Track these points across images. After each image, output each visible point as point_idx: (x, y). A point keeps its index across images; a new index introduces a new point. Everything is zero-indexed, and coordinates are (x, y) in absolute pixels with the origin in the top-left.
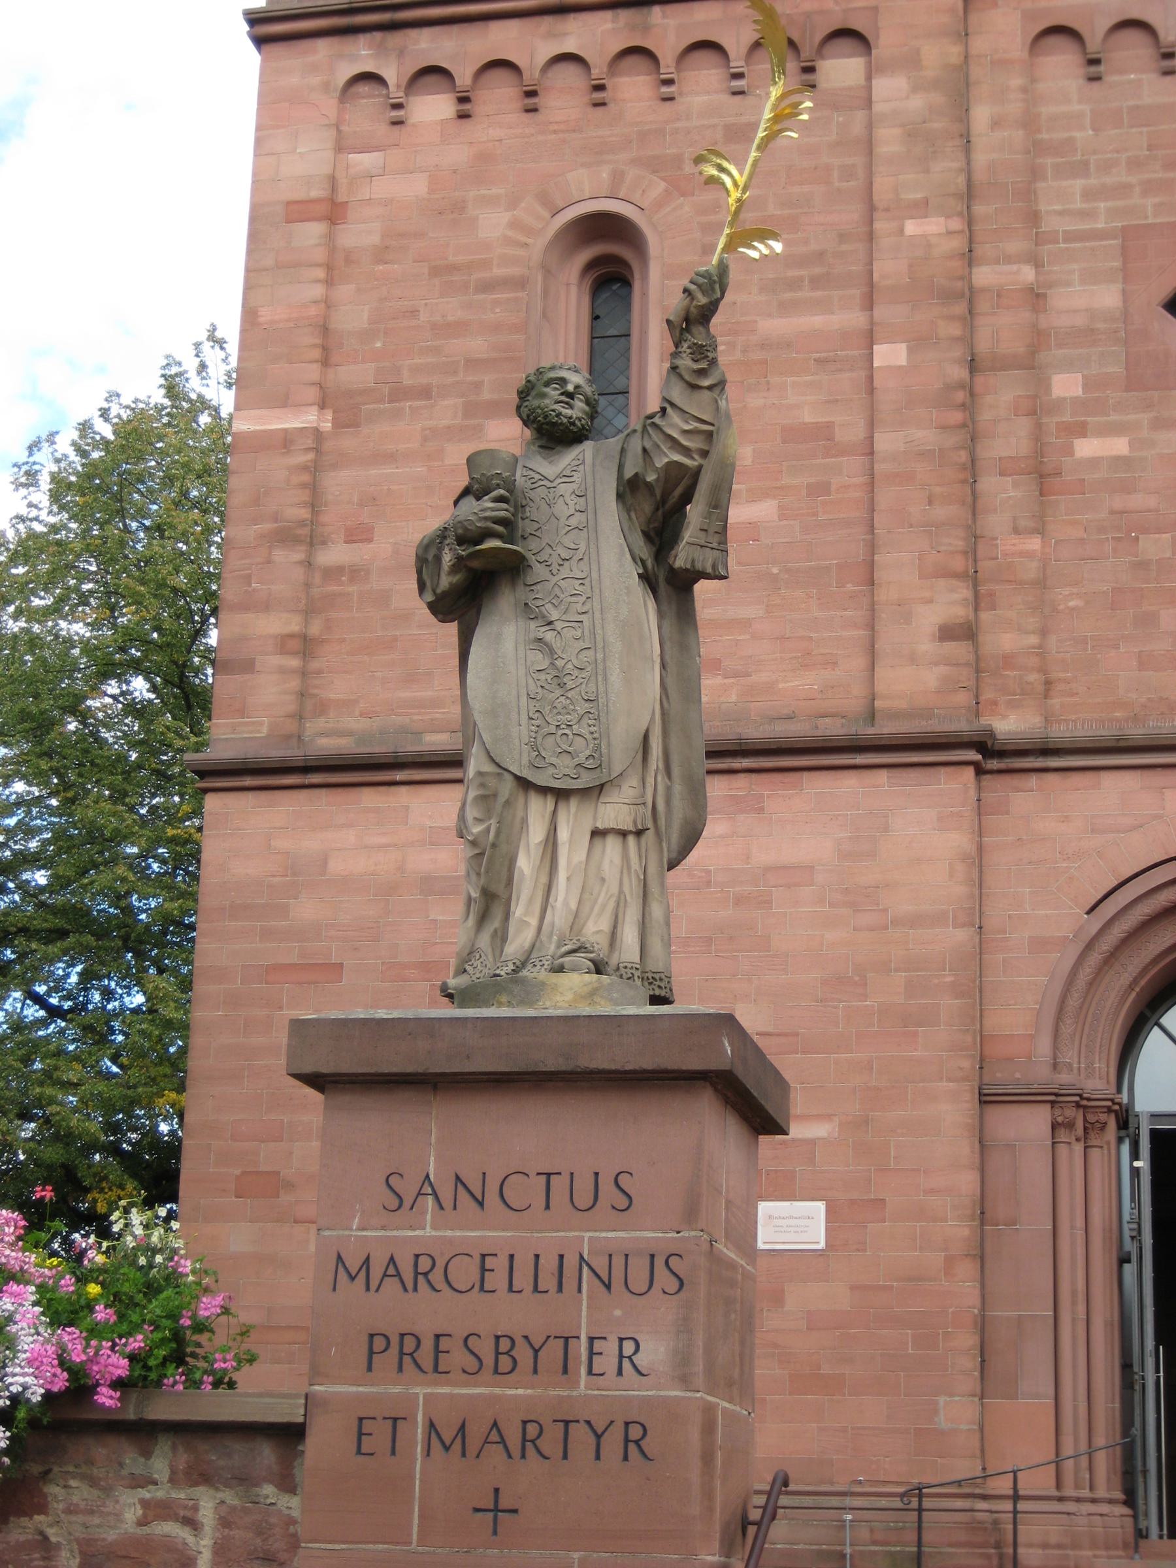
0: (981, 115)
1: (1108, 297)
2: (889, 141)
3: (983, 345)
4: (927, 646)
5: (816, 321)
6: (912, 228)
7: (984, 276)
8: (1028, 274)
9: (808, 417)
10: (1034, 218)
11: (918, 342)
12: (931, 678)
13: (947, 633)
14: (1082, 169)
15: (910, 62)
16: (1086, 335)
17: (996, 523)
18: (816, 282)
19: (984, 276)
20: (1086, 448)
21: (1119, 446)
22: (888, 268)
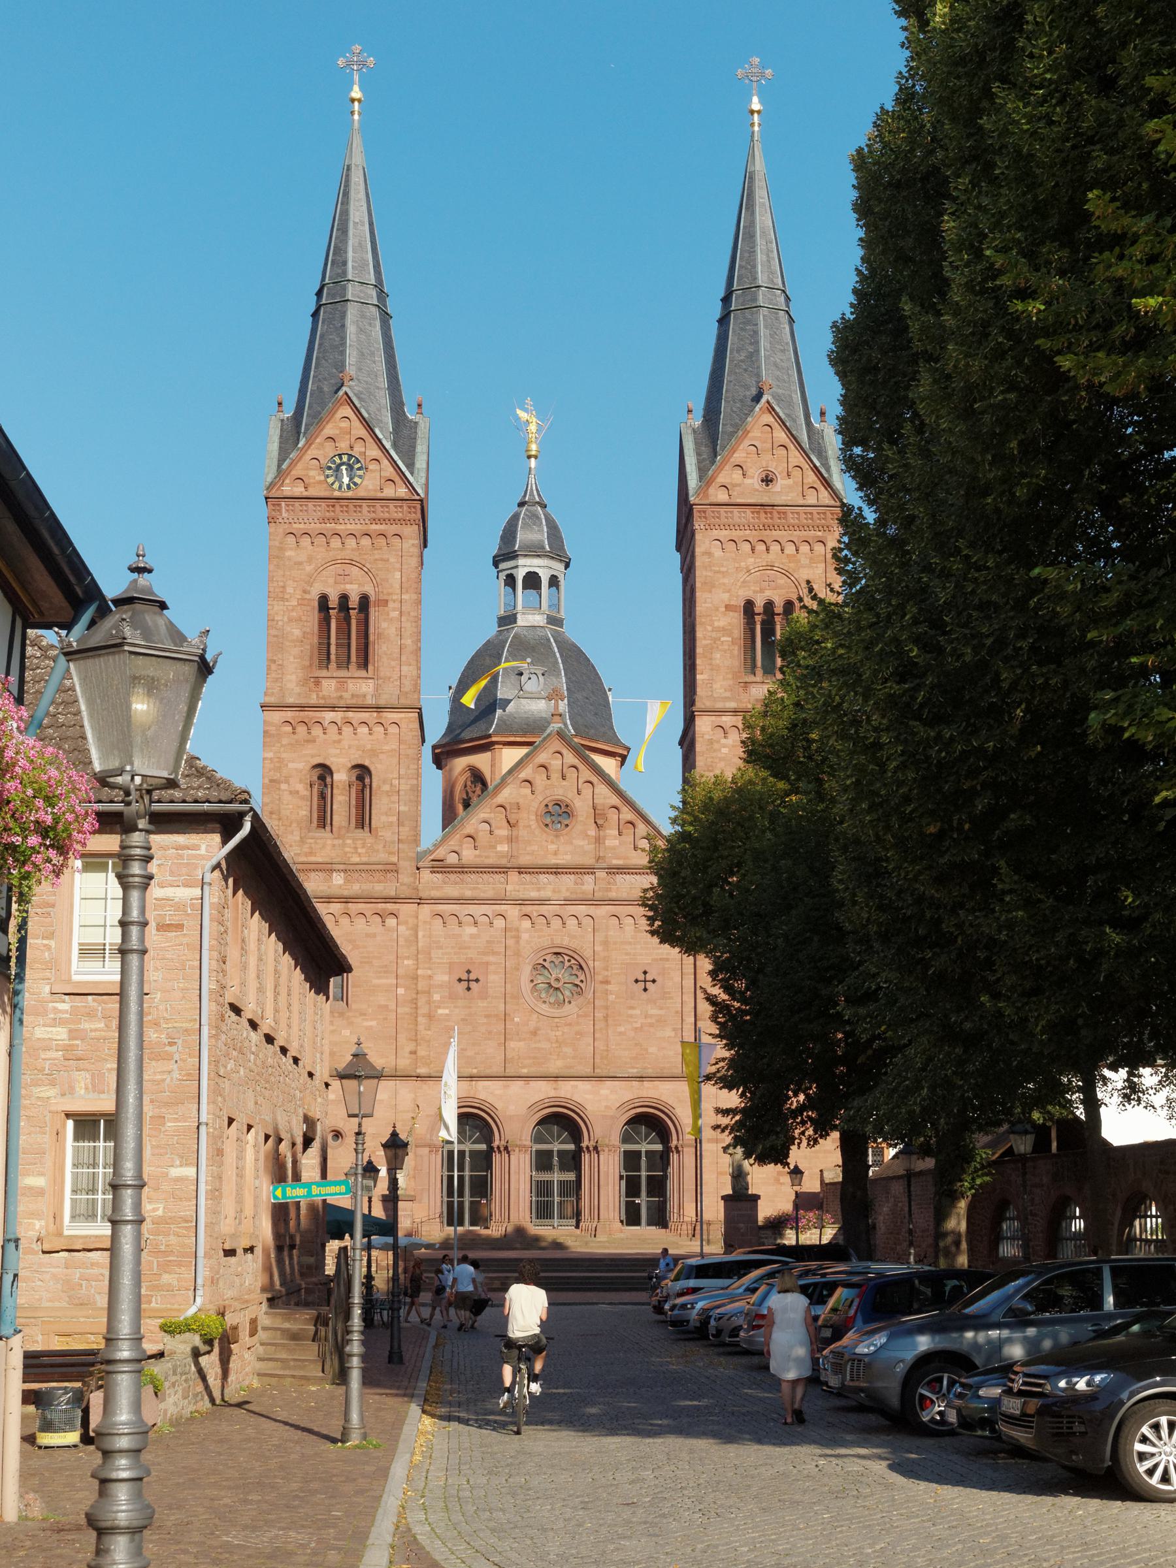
0: (420, 934)
1: (446, 978)
2: (401, 941)
3: (420, 988)
4: (407, 1055)
5: (384, 981)
6: (406, 962)
7: (420, 972)
8: (429, 972)
9: (383, 1003)
10: (430, 959)
11: (407, 988)
12: (407, 1062)
13: (411, 1053)
14: (441, 948)
15: (406, 923)
16: (441, 986)
17: (421, 1028)
18: (385, 972)
19: (420, 972)
20: (440, 1011)
21: (447, 1011)
22: (401, 971)
